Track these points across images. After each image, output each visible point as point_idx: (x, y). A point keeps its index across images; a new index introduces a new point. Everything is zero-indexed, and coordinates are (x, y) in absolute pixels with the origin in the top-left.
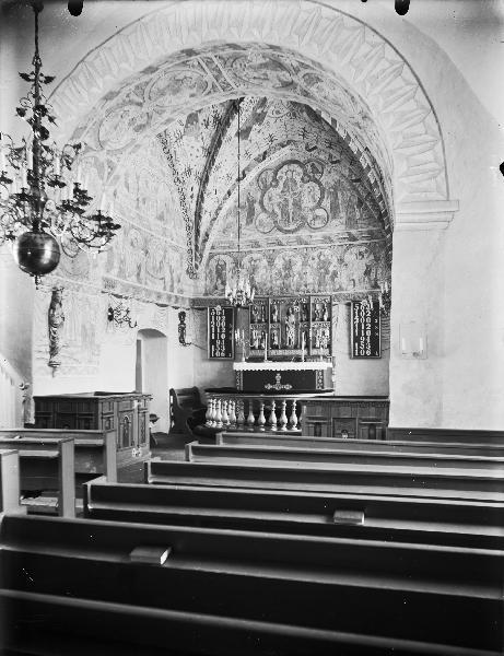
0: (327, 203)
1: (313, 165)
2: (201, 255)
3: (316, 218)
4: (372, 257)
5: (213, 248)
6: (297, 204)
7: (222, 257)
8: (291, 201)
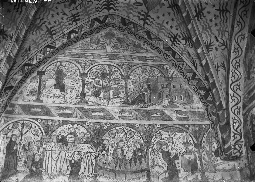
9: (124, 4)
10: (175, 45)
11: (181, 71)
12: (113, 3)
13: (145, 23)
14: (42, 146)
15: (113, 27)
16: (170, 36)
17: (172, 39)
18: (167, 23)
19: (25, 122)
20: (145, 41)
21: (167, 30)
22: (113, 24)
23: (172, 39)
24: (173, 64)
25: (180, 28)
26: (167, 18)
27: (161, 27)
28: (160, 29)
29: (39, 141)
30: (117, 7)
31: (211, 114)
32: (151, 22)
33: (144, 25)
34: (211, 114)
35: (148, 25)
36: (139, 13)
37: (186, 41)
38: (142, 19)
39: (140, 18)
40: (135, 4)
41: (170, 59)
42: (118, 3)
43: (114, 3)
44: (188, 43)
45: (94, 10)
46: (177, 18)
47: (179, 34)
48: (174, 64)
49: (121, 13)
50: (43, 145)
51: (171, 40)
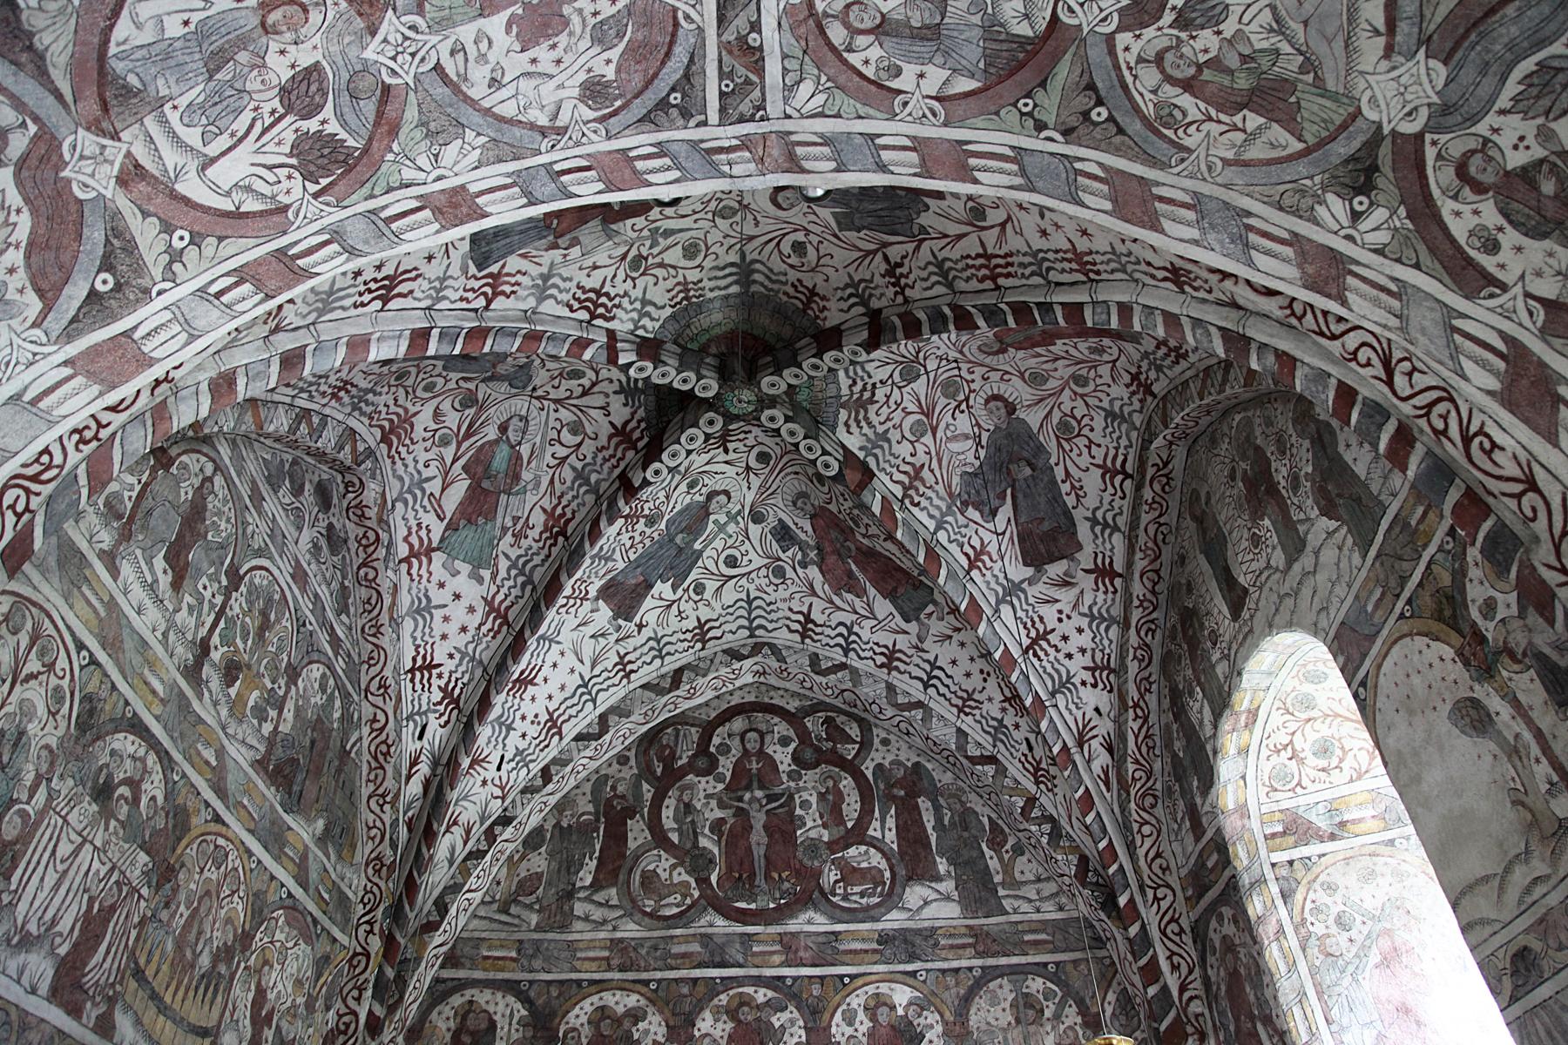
0: (885, 829)
1: (828, 721)
2: (401, 982)
3: (850, 874)
4: (1072, 1016)
5: (451, 960)
6: (783, 827)
7: (483, 997)
8: (759, 819)
10: (412, 680)
11: (381, 758)
13: (406, 560)
14: (49, 780)
15: (346, 487)
16: (422, 652)
17: (419, 662)
18: (446, 619)
19: (47, 620)
20: (373, 602)
21: (427, 630)
22: (357, 481)
23: (419, 662)
24: (375, 720)
25: (460, 664)
26: (458, 613)
28: (418, 611)
29: (51, 751)
31: (376, 930)
34: (376, 930)
35: (409, 573)
36: (419, 525)
37: (443, 699)
38: (411, 546)
41: (381, 704)
44: (442, 708)
45: (369, 409)
47: (445, 670)
48: (377, 726)
50: (55, 780)
51: (414, 659)
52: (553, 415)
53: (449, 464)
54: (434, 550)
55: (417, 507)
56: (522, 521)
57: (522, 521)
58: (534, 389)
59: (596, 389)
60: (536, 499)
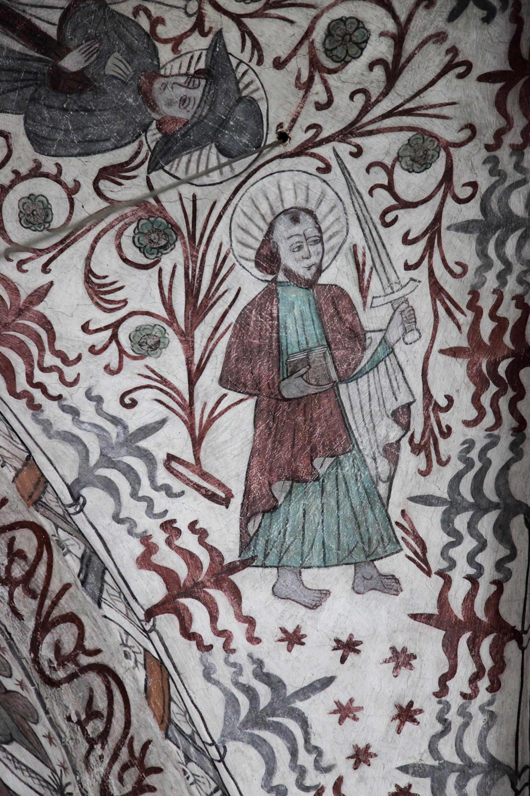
9: (99, 411)
12: (34, 350)
20: (101, 704)
27: (271, 710)
30: (41, 386)
32: (220, 634)
33: (150, 613)
39: (156, 559)
40: (174, 465)
42: (69, 379)
43: (41, 356)
46: (452, 716)
49: (42, 439)
52: (351, 163)
53: (182, 385)
54: (233, 568)
55: (146, 489)
56: (417, 410)
57: (417, 410)
58: (283, 137)
59: (409, 46)
60: (421, 348)
